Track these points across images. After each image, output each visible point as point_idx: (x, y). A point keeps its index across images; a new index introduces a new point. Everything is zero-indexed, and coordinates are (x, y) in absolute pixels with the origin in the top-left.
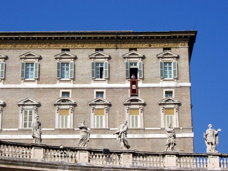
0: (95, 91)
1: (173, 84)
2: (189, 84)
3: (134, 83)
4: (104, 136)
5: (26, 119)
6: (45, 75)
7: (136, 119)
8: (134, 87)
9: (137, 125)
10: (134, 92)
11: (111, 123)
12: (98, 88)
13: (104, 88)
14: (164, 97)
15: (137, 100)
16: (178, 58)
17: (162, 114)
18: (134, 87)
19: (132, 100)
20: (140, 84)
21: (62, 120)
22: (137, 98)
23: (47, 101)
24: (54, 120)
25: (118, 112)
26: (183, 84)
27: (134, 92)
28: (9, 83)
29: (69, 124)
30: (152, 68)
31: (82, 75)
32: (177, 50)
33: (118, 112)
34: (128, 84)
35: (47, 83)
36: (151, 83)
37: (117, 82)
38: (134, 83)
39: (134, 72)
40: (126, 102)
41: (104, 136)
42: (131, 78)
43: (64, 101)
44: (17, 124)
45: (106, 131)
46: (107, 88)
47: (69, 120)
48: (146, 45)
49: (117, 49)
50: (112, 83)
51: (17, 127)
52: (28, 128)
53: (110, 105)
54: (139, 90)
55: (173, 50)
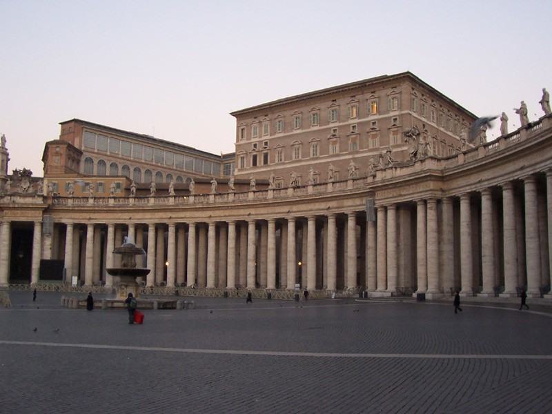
1: (397, 113)
4: (357, 156)
16: (400, 93)
17: (391, 136)
19: (372, 129)
26: (403, 112)
37: (364, 118)
40: (368, 130)
41: (357, 156)
43: (334, 135)
45: (358, 152)
46: (359, 123)
48: (381, 88)
49: (363, 94)
51: (309, 156)
53: (359, 134)
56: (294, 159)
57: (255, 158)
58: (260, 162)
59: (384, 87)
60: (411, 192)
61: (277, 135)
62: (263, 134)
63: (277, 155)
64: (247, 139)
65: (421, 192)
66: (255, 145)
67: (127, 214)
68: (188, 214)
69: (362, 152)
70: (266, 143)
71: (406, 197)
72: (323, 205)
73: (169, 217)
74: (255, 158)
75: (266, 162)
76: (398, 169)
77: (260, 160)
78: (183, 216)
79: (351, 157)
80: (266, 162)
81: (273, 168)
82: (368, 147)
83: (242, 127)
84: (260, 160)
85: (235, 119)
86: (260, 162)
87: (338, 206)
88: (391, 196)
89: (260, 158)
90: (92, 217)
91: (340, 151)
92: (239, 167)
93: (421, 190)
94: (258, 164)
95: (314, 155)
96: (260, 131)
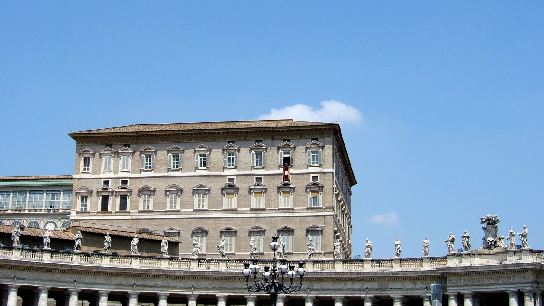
0: (255, 177)
1: (318, 170)
2: (331, 170)
3: (286, 169)
5: (199, 200)
6: (215, 164)
7: (288, 200)
8: (286, 173)
9: (288, 205)
10: (286, 177)
11: (268, 204)
12: (257, 175)
13: (262, 175)
14: (311, 181)
15: (289, 185)
18: (286, 173)
19: (284, 185)
20: (291, 171)
21: (228, 202)
22: (288, 182)
23: (216, 186)
24: (221, 202)
25: (273, 194)
26: (327, 170)
27: (286, 177)
28: (186, 171)
29: (233, 205)
30: (302, 156)
31: (245, 163)
32: (323, 140)
33: (273, 194)
34: (281, 171)
35: (216, 171)
36: (300, 169)
37: (273, 169)
38: (286, 169)
39: (287, 160)
42: (284, 165)
44: (193, 205)
46: (265, 175)
47: (233, 201)
49: (273, 140)
50: (269, 170)
52: (201, 208)
54: (290, 176)
55: (320, 140)
56: (168, 208)
57: (105, 200)
58: (114, 205)
59: (301, 137)
60: (501, 281)
61: (143, 174)
62: (120, 169)
63: (141, 200)
64: (94, 173)
65: (517, 283)
66: (106, 183)
67: (70, 276)
68: (160, 282)
69: (270, 211)
70: (124, 182)
71: (494, 287)
72: (358, 286)
73: (132, 283)
74: (105, 200)
75: (123, 206)
76: (476, 256)
77: (114, 203)
78: (152, 284)
79: (254, 215)
80: (123, 206)
81: (134, 217)
82: (278, 205)
83: (87, 156)
84: (114, 203)
85: (74, 142)
86: (114, 205)
87: (380, 287)
88: (470, 283)
89: (114, 202)
90: (17, 275)
91: (238, 205)
92: (79, 209)
93: (516, 280)
94: (110, 209)
95: (199, 207)
96: (116, 166)
